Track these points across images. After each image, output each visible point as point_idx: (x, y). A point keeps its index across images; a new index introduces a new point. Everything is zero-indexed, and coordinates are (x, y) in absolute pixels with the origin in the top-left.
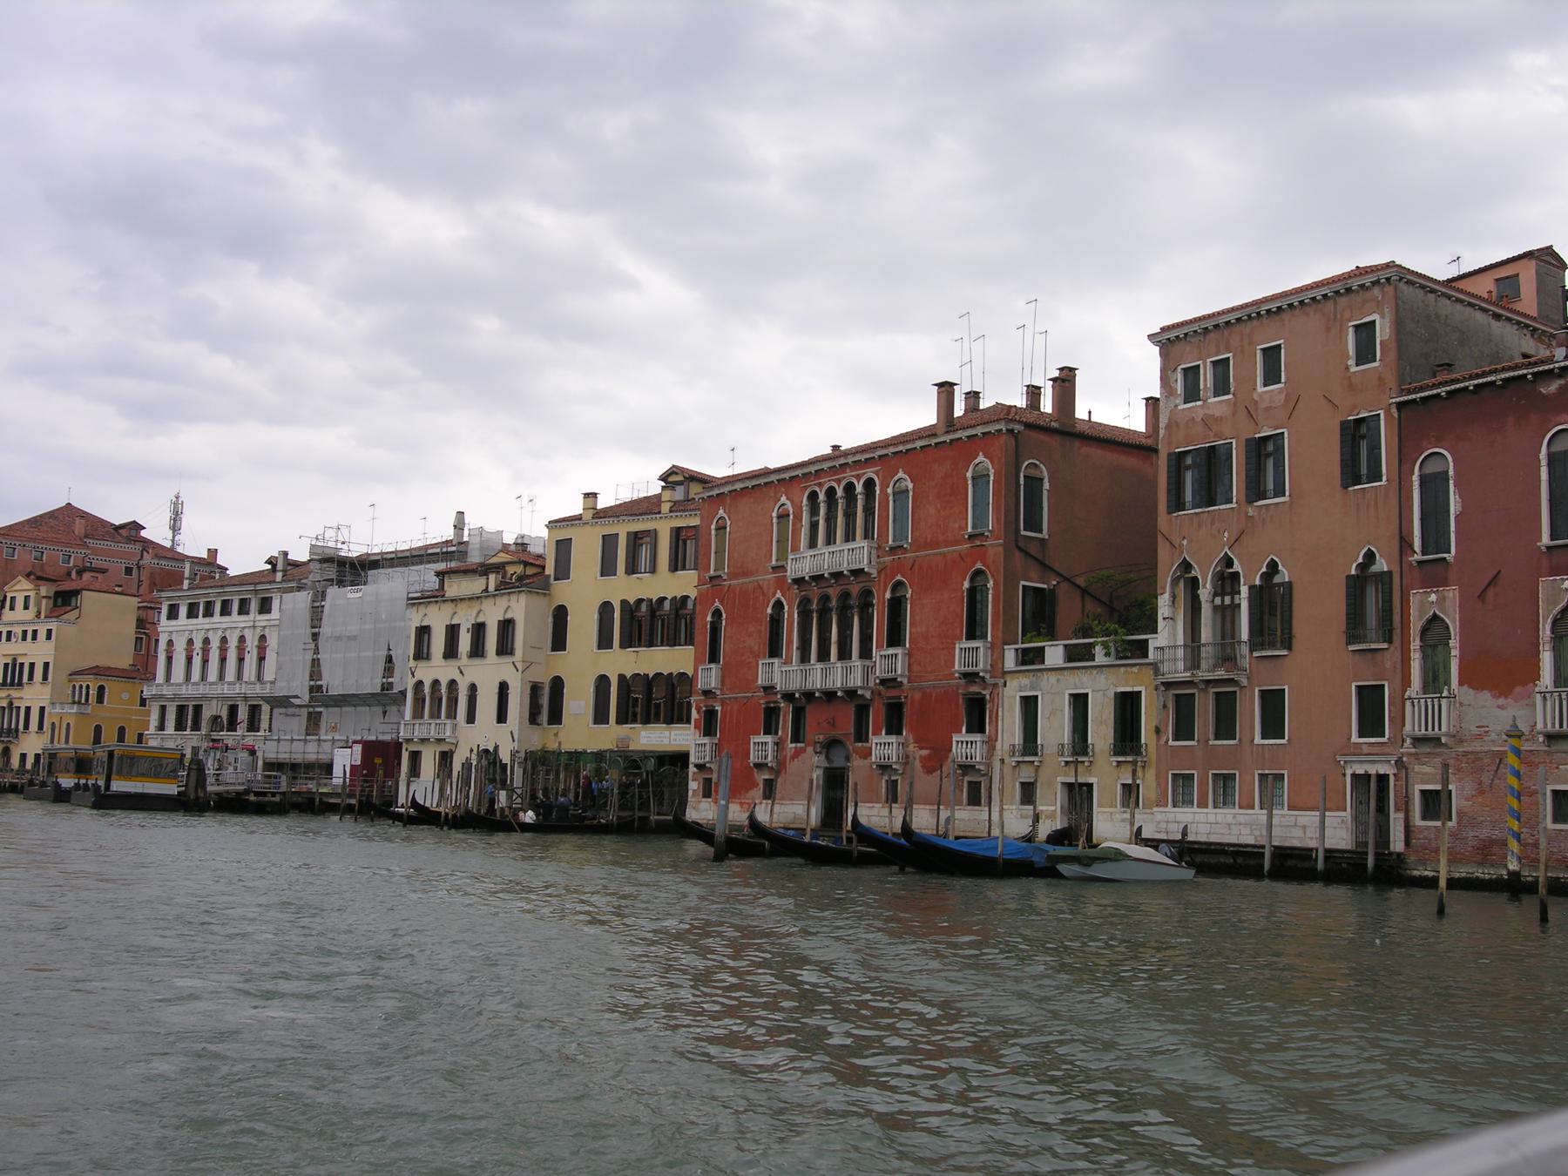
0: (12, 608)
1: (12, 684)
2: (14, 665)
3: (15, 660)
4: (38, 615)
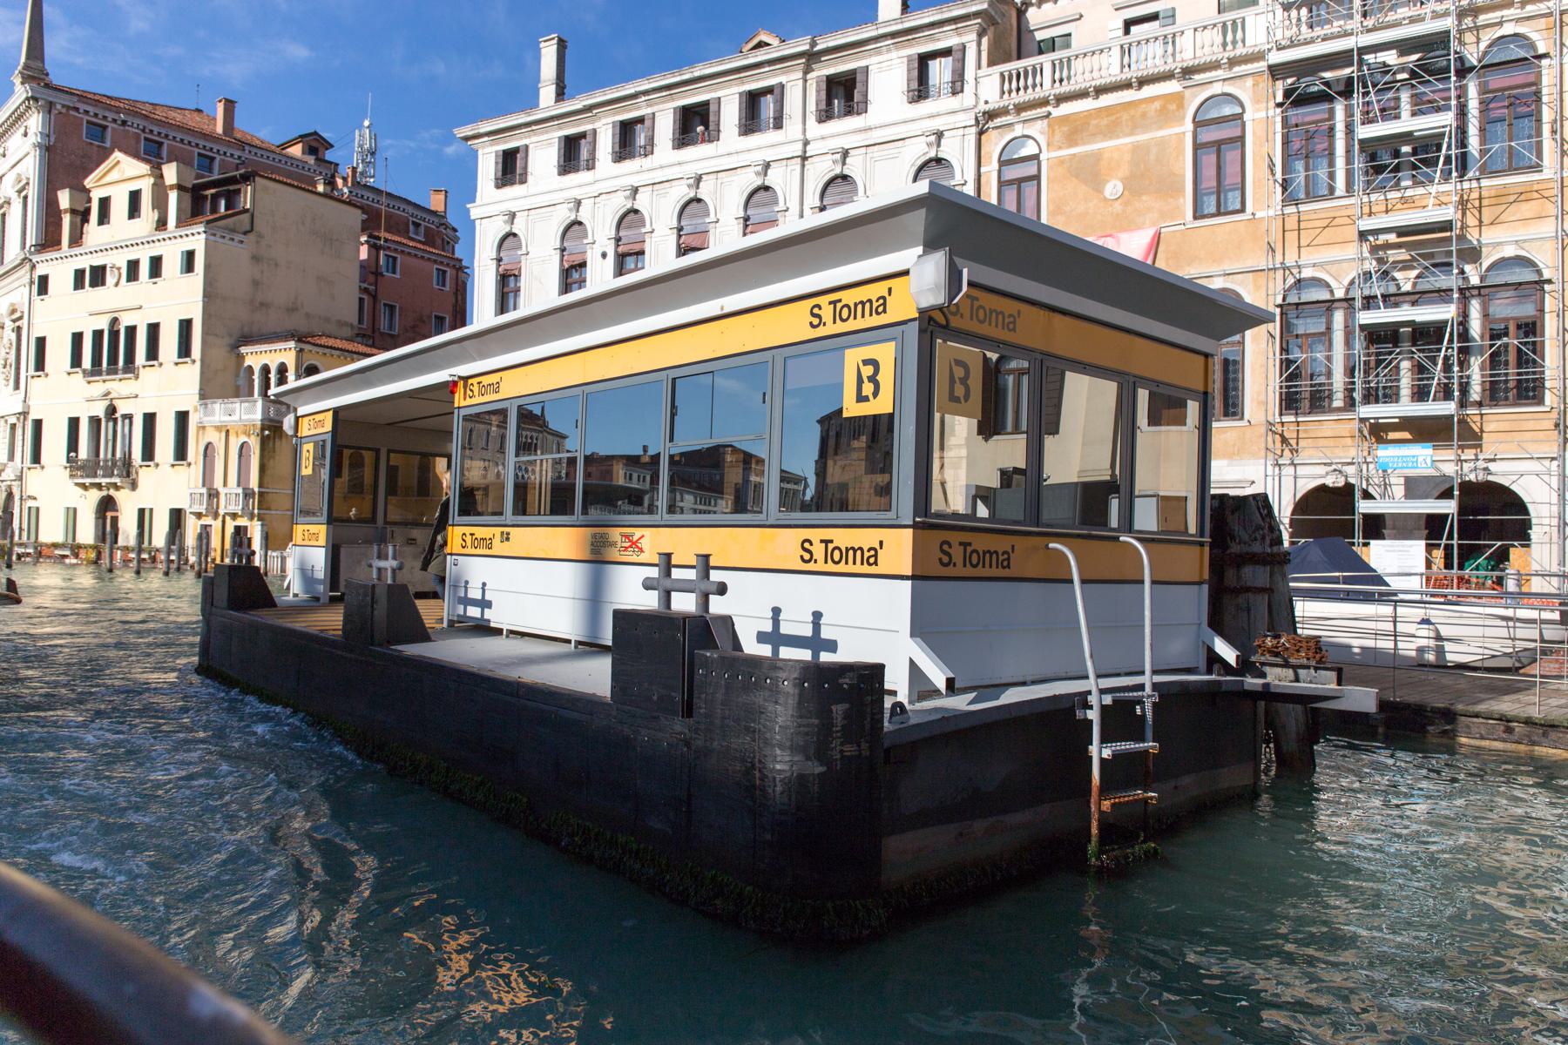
0: (104, 218)
1: (113, 370)
2: (114, 335)
3: (115, 321)
4: (162, 224)
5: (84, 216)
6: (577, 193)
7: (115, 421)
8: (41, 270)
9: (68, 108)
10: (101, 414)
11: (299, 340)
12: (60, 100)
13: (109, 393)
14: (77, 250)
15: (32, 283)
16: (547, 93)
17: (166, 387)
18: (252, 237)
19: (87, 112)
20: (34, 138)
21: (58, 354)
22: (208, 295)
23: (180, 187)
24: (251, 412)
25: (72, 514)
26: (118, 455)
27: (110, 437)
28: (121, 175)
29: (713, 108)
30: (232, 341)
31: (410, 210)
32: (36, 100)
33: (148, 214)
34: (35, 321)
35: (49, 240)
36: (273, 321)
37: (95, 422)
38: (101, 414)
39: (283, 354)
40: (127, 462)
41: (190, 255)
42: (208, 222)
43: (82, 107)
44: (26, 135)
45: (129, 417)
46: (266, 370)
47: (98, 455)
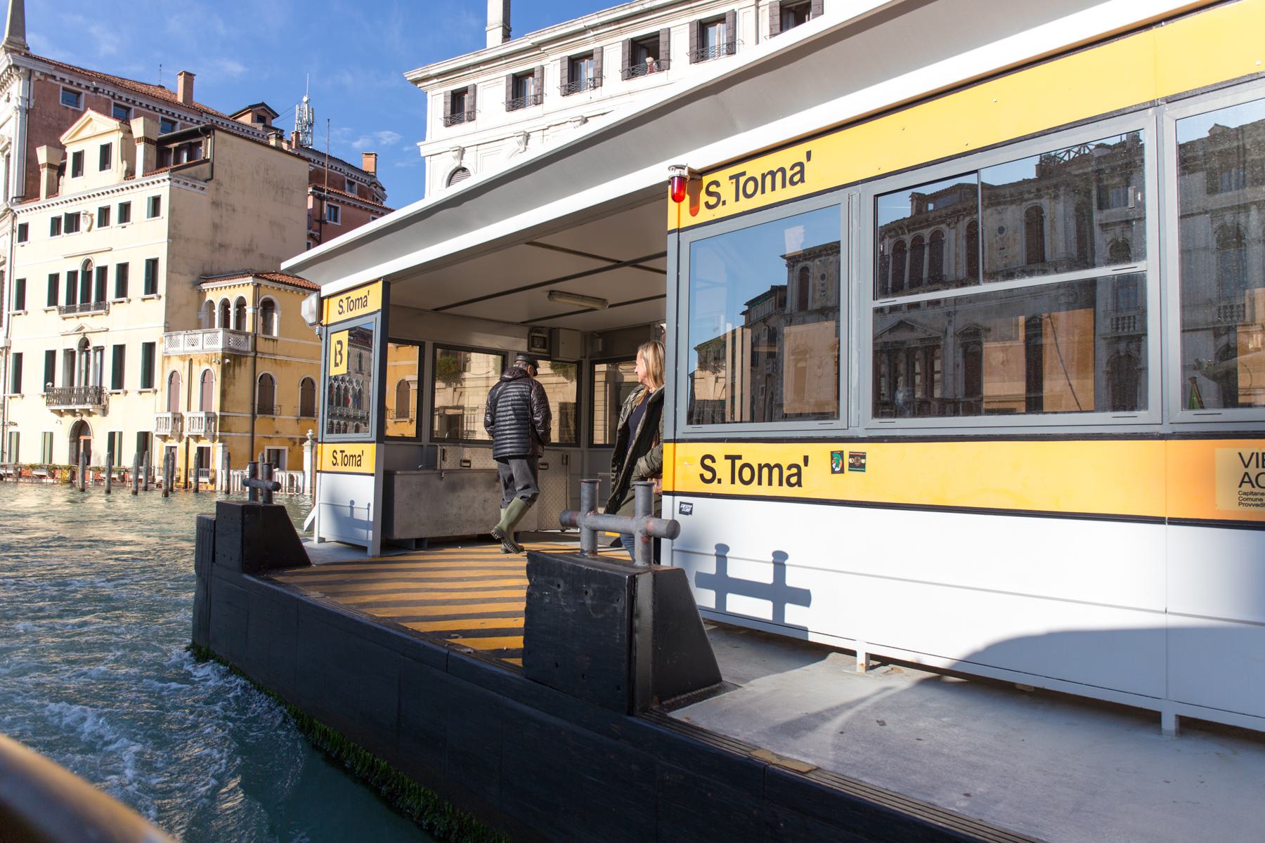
0: (78, 170)
2: (87, 275)
3: (88, 262)
4: (130, 174)
5: (61, 170)
6: (526, 127)
7: (88, 352)
8: (21, 219)
9: (46, 75)
10: (76, 348)
11: (257, 276)
12: (39, 68)
13: (82, 328)
14: (53, 200)
15: (13, 231)
16: (494, 35)
17: (134, 321)
18: (211, 184)
19: (62, 80)
20: (15, 102)
21: (37, 294)
22: (172, 236)
23: (147, 140)
24: (213, 342)
25: (49, 438)
26: (91, 383)
27: (83, 368)
28: (93, 130)
29: (662, 38)
30: (194, 278)
31: (346, 170)
32: (17, 68)
33: (118, 165)
34: (16, 265)
35: (29, 193)
36: (230, 260)
37: (70, 354)
38: (76, 348)
39: (242, 289)
40: (99, 391)
41: (156, 201)
42: (172, 170)
43: (59, 75)
44: (8, 100)
45: (100, 349)
46: (225, 304)
47: (72, 383)
